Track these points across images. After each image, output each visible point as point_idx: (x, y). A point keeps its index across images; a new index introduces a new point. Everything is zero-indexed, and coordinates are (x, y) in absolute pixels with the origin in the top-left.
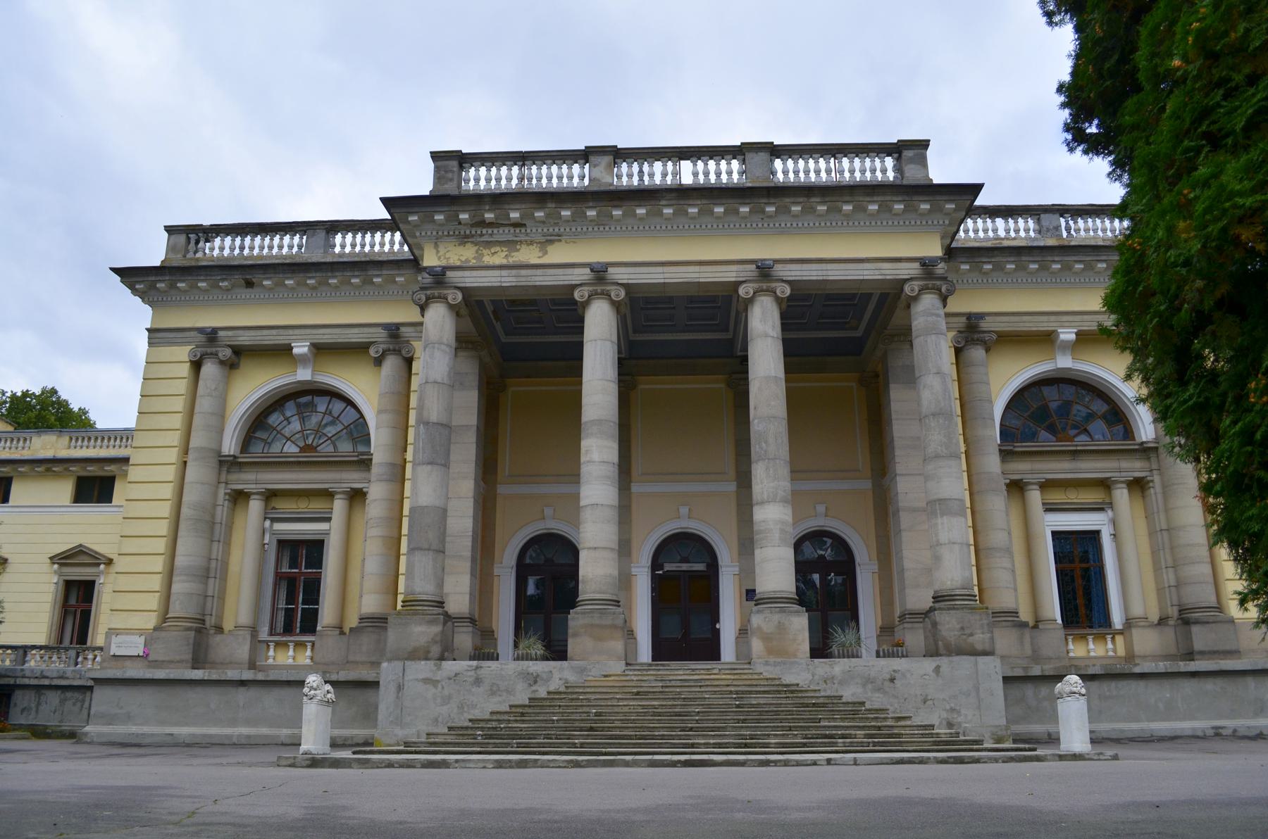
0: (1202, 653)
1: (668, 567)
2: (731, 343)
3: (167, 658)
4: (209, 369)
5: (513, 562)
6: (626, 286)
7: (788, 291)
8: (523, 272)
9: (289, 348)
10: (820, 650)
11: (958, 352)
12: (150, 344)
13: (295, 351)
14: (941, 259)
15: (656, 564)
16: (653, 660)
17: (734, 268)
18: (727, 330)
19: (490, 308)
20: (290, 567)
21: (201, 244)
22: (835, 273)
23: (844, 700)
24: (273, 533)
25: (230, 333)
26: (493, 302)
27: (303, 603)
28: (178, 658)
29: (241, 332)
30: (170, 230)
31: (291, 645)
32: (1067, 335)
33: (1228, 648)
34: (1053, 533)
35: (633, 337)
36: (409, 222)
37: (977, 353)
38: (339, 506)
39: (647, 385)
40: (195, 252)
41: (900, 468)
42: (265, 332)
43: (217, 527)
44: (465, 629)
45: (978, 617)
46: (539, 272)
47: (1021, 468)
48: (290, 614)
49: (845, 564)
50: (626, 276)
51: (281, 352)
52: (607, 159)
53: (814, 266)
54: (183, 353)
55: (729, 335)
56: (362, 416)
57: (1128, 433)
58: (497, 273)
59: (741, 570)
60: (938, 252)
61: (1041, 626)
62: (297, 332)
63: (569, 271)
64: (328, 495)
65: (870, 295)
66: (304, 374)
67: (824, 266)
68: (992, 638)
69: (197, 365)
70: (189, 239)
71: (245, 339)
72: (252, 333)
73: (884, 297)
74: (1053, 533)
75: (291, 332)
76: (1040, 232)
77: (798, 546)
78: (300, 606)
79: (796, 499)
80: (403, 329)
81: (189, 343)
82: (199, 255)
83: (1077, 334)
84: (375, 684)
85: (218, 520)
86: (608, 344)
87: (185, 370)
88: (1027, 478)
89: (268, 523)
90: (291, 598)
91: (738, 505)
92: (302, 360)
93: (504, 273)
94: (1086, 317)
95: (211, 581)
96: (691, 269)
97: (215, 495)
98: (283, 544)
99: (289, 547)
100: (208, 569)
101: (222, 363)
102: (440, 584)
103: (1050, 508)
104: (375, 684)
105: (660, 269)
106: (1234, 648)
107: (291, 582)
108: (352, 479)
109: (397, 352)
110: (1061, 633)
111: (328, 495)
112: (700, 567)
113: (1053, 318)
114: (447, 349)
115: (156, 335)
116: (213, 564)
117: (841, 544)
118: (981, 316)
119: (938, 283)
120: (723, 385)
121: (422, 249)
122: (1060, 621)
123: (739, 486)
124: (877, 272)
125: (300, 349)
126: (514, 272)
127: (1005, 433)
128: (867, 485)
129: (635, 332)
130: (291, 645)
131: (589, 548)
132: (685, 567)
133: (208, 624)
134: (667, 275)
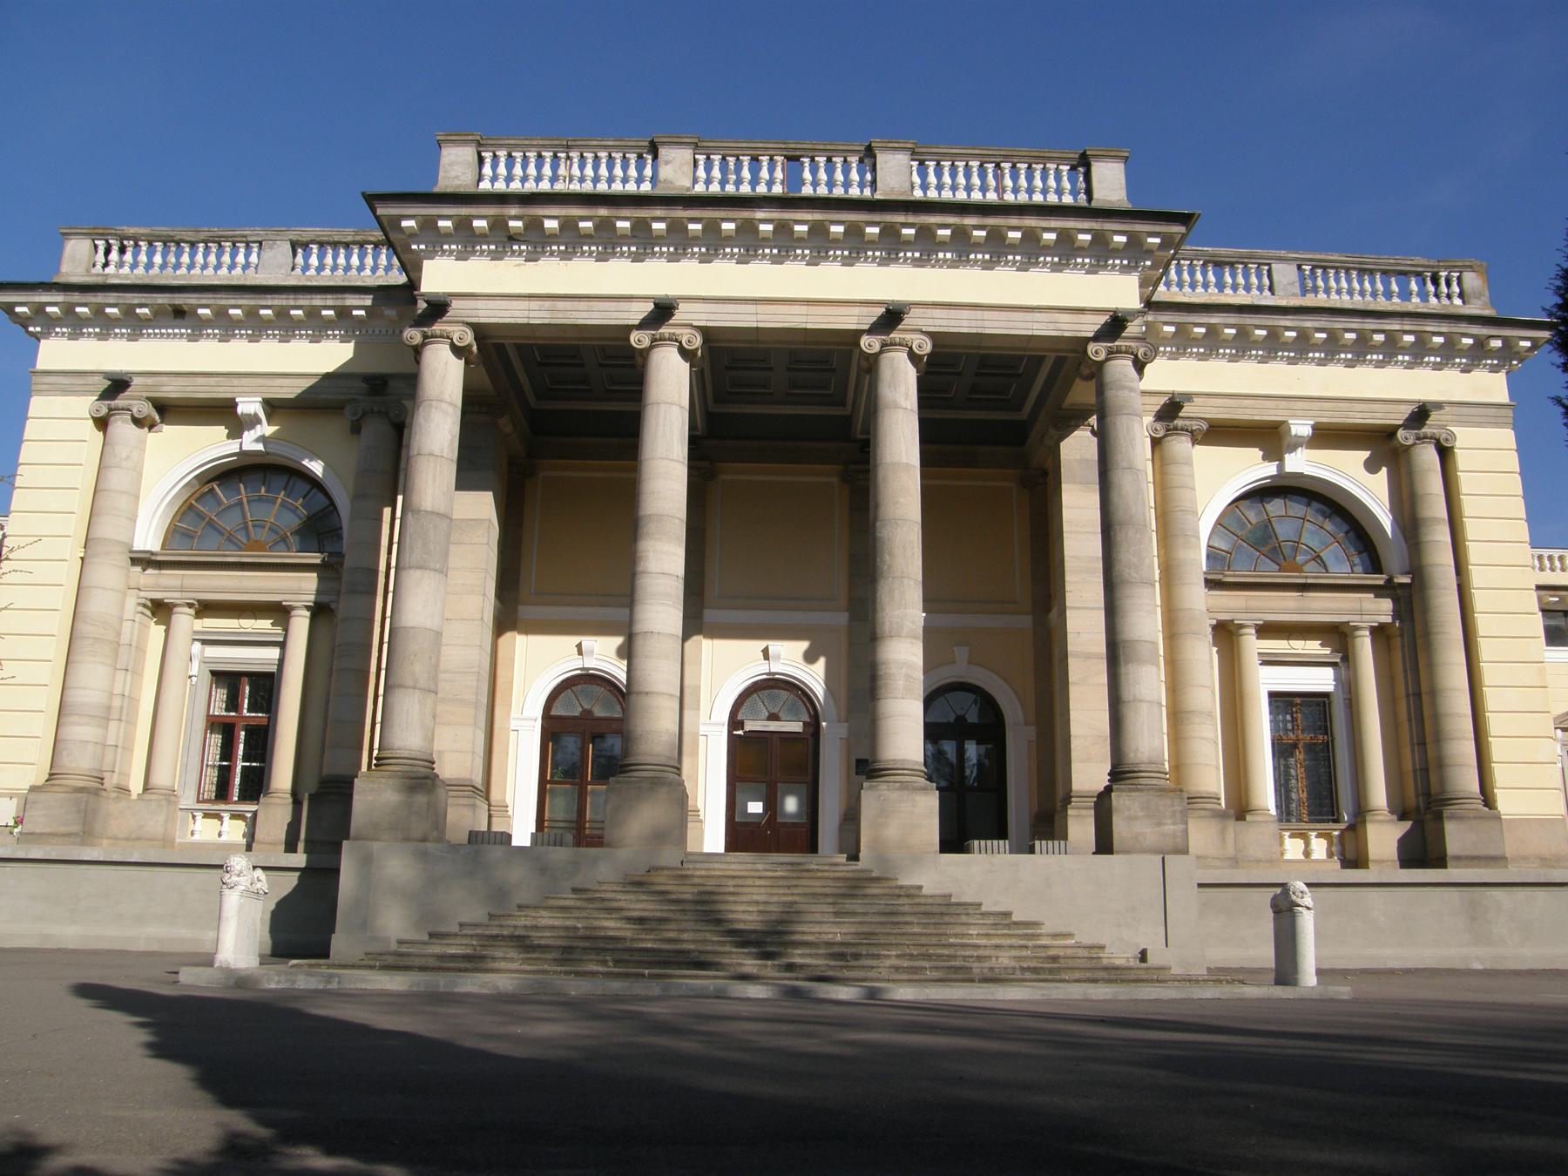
0: (1458, 858)
1: (750, 726)
2: (847, 421)
3: (48, 830)
4: (122, 428)
5: (539, 713)
6: (707, 333)
7: (927, 347)
8: (561, 305)
9: (231, 405)
10: (954, 840)
11: (1156, 443)
13: (239, 410)
14: (1139, 312)
15: (734, 722)
17: (856, 310)
18: (843, 404)
19: (513, 355)
20: (227, 710)
21: (114, 256)
22: (995, 325)
23: (984, 909)
24: (204, 661)
25: (150, 381)
26: (518, 347)
27: (244, 760)
28: (63, 829)
29: (165, 379)
31: (226, 816)
32: (1301, 428)
33: (1492, 852)
34: (1273, 695)
35: (713, 409)
36: (401, 230)
37: (1180, 446)
39: (732, 474)
40: (106, 265)
41: (1071, 599)
42: (200, 380)
43: (123, 650)
45: (1169, 802)
46: (582, 305)
47: (1231, 604)
48: (224, 776)
49: (991, 728)
50: (704, 316)
53: (966, 314)
54: (85, 405)
55: (848, 410)
56: (332, 503)
57: (1375, 566)
58: (524, 304)
60: (1135, 303)
61: (1248, 818)
62: (245, 381)
65: (1041, 359)
67: (979, 314)
68: (1186, 832)
70: (96, 247)
72: (182, 381)
73: (1060, 362)
74: (1273, 695)
75: (235, 381)
76: (1271, 289)
77: (929, 702)
78: (240, 764)
79: (931, 637)
80: (392, 383)
81: (91, 393)
82: (111, 270)
83: (1315, 428)
85: (124, 639)
86: (676, 409)
88: (1239, 619)
89: (197, 645)
90: (227, 751)
93: (534, 304)
94: (1327, 405)
95: (113, 725)
96: (797, 309)
97: (122, 605)
98: (222, 677)
99: (226, 679)
100: (109, 708)
102: (430, 739)
103: (1269, 661)
105: (751, 308)
106: (1499, 853)
107: (226, 730)
110: (1274, 827)
111: (279, 612)
112: (796, 727)
113: (1283, 404)
114: (450, 409)
116: (117, 702)
117: (988, 703)
118: (1189, 397)
119: (1133, 344)
120: (835, 480)
121: (419, 269)
122: (1273, 811)
123: (852, 619)
124: (1052, 326)
125: (249, 405)
126: (548, 304)
127: (1212, 556)
128: (1026, 621)
129: (717, 401)
130: (226, 816)
132: (773, 726)
133: (107, 784)
134: (760, 317)
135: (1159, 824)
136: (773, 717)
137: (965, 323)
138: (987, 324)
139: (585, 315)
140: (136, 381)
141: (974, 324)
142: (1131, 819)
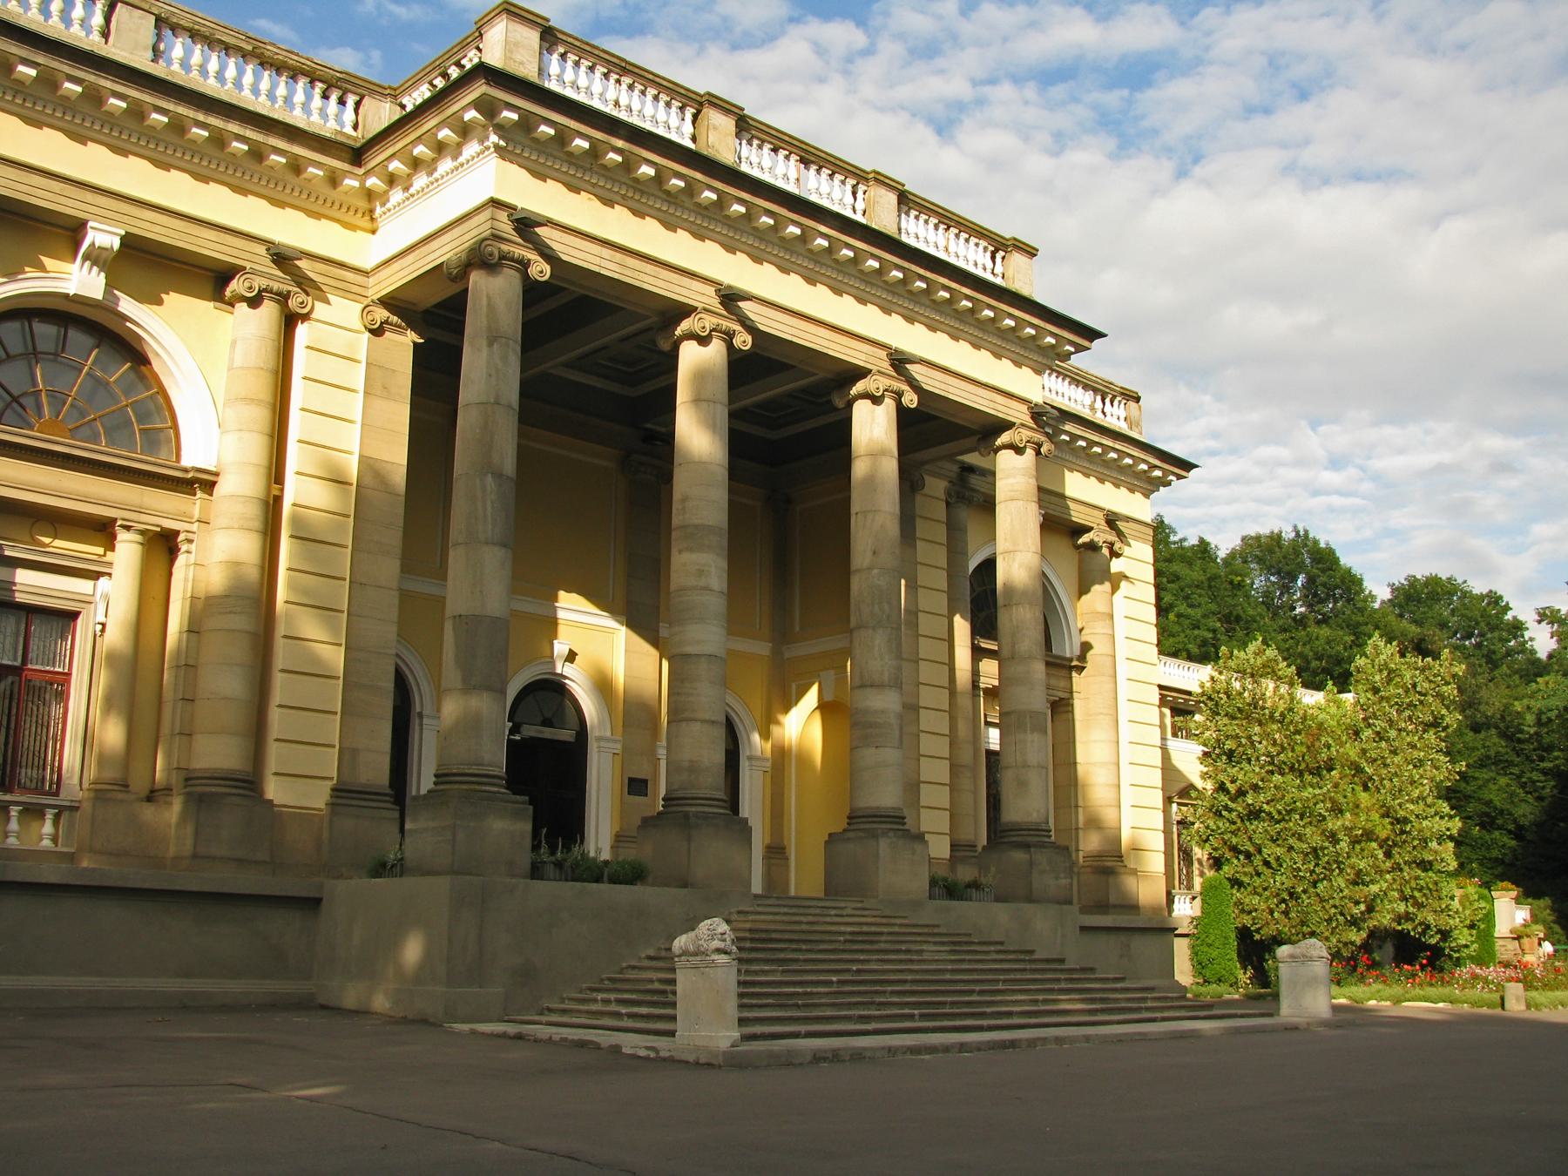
0: (1115, 906)
1: (529, 731)
16: (826, 894)
31: (14, 811)
38: (127, 553)
44: (388, 814)
46: (649, 268)
59: (624, 749)
63: (686, 281)
64: (102, 530)
84: (317, 902)
93: (607, 253)
104: (317, 902)
108: (163, 508)
109: (283, 298)
111: (102, 530)
125: (102, 236)
126: (618, 256)
128: (763, 649)
131: (704, 721)
137: (937, 384)
138: (951, 390)
139: (651, 280)
141: (943, 387)
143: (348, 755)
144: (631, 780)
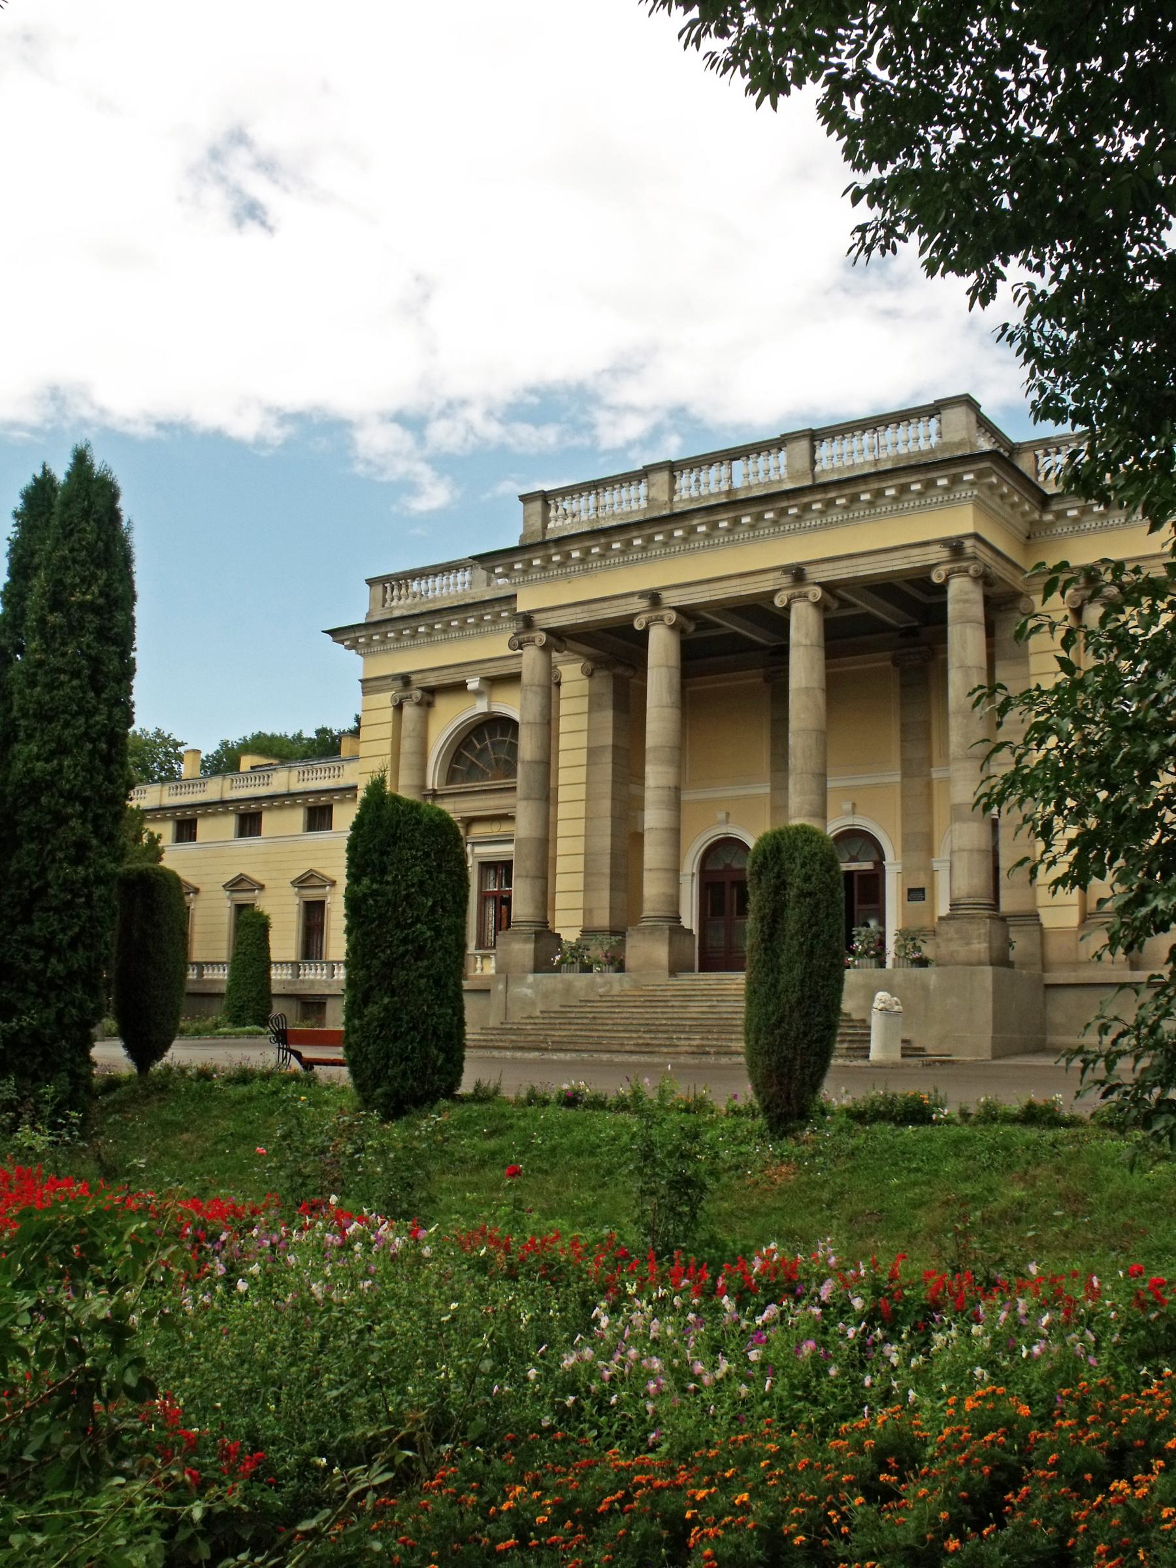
4: (409, 711)
8: (594, 606)
12: (364, 693)
13: (470, 687)
25: (420, 676)
30: (371, 582)
42: (446, 671)
51: (459, 687)
52: (664, 476)
62: (470, 668)
66: (481, 706)
69: (399, 707)
71: (432, 680)
72: (436, 673)
87: (388, 715)
91: (903, 797)
92: (477, 693)
93: (578, 609)
101: (419, 704)
105: (705, 587)
112: (868, 866)
114: (539, 690)
115: (369, 685)
125: (473, 684)
126: (586, 607)
132: (854, 866)
135: (968, 944)
136: (854, 859)
140: (414, 677)
142: (951, 940)
143: (588, 912)
144: (910, 891)
